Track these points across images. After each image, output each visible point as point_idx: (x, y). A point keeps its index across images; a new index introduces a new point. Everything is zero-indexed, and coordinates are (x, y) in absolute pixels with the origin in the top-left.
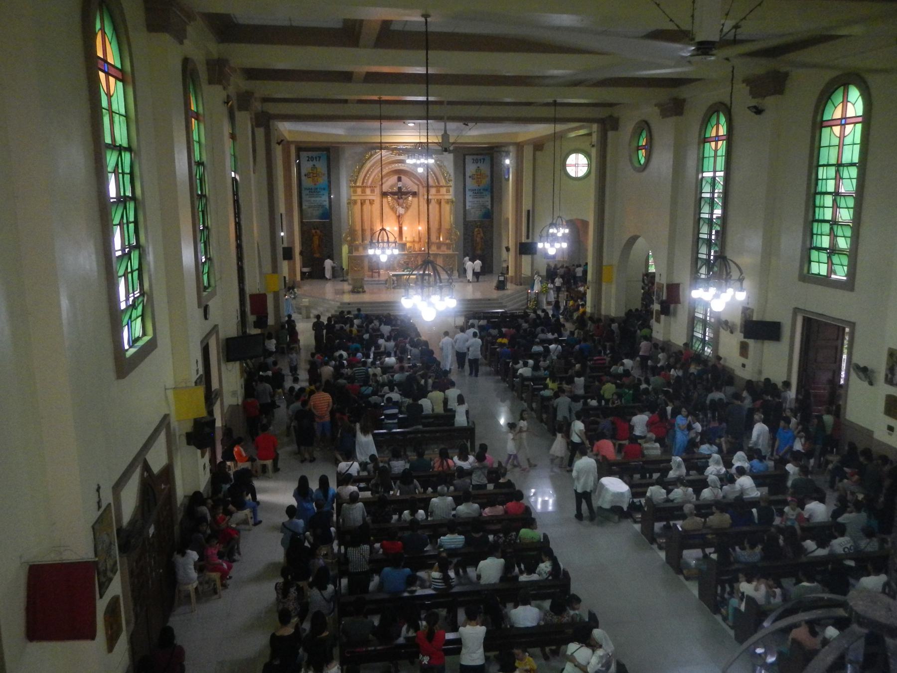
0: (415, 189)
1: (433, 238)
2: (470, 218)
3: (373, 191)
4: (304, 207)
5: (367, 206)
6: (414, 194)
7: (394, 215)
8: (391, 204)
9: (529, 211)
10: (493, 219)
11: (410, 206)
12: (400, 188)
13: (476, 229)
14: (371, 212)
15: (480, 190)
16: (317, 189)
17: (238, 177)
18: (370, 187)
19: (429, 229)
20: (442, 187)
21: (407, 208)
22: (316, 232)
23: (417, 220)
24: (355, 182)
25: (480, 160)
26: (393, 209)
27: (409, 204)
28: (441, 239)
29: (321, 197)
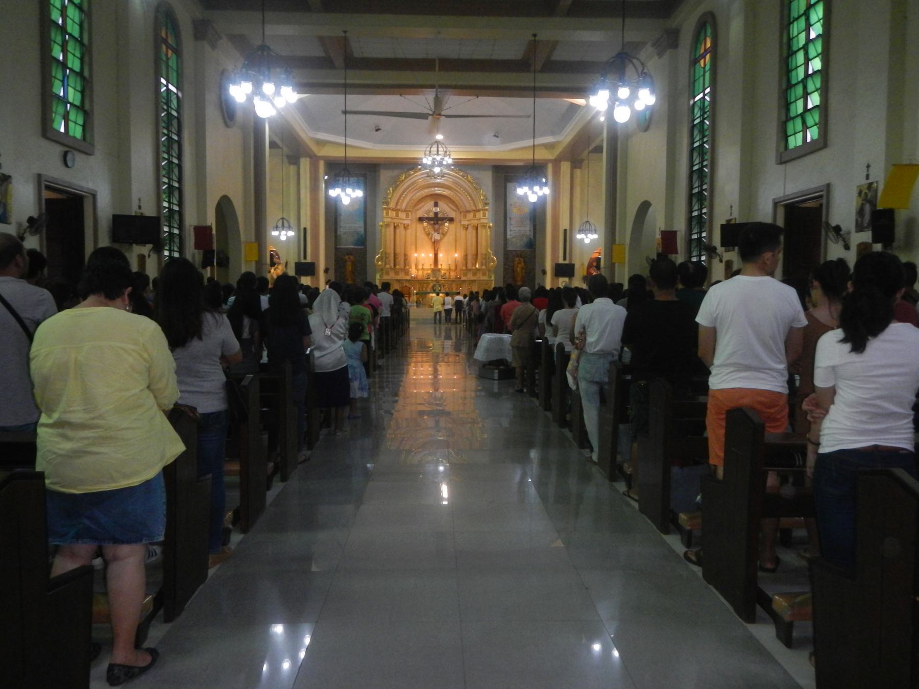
0: (452, 214)
1: (469, 266)
2: (510, 248)
3: (407, 216)
4: (339, 233)
5: (400, 231)
6: (451, 220)
8: (426, 230)
9: (565, 231)
10: (535, 248)
11: (447, 232)
12: (436, 214)
13: (517, 259)
14: (405, 237)
17: (180, 95)
18: (405, 211)
19: (466, 256)
20: (479, 211)
21: (444, 235)
22: (349, 258)
23: (454, 247)
24: (388, 205)
26: (428, 234)
27: (446, 231)
28: (477, 266)
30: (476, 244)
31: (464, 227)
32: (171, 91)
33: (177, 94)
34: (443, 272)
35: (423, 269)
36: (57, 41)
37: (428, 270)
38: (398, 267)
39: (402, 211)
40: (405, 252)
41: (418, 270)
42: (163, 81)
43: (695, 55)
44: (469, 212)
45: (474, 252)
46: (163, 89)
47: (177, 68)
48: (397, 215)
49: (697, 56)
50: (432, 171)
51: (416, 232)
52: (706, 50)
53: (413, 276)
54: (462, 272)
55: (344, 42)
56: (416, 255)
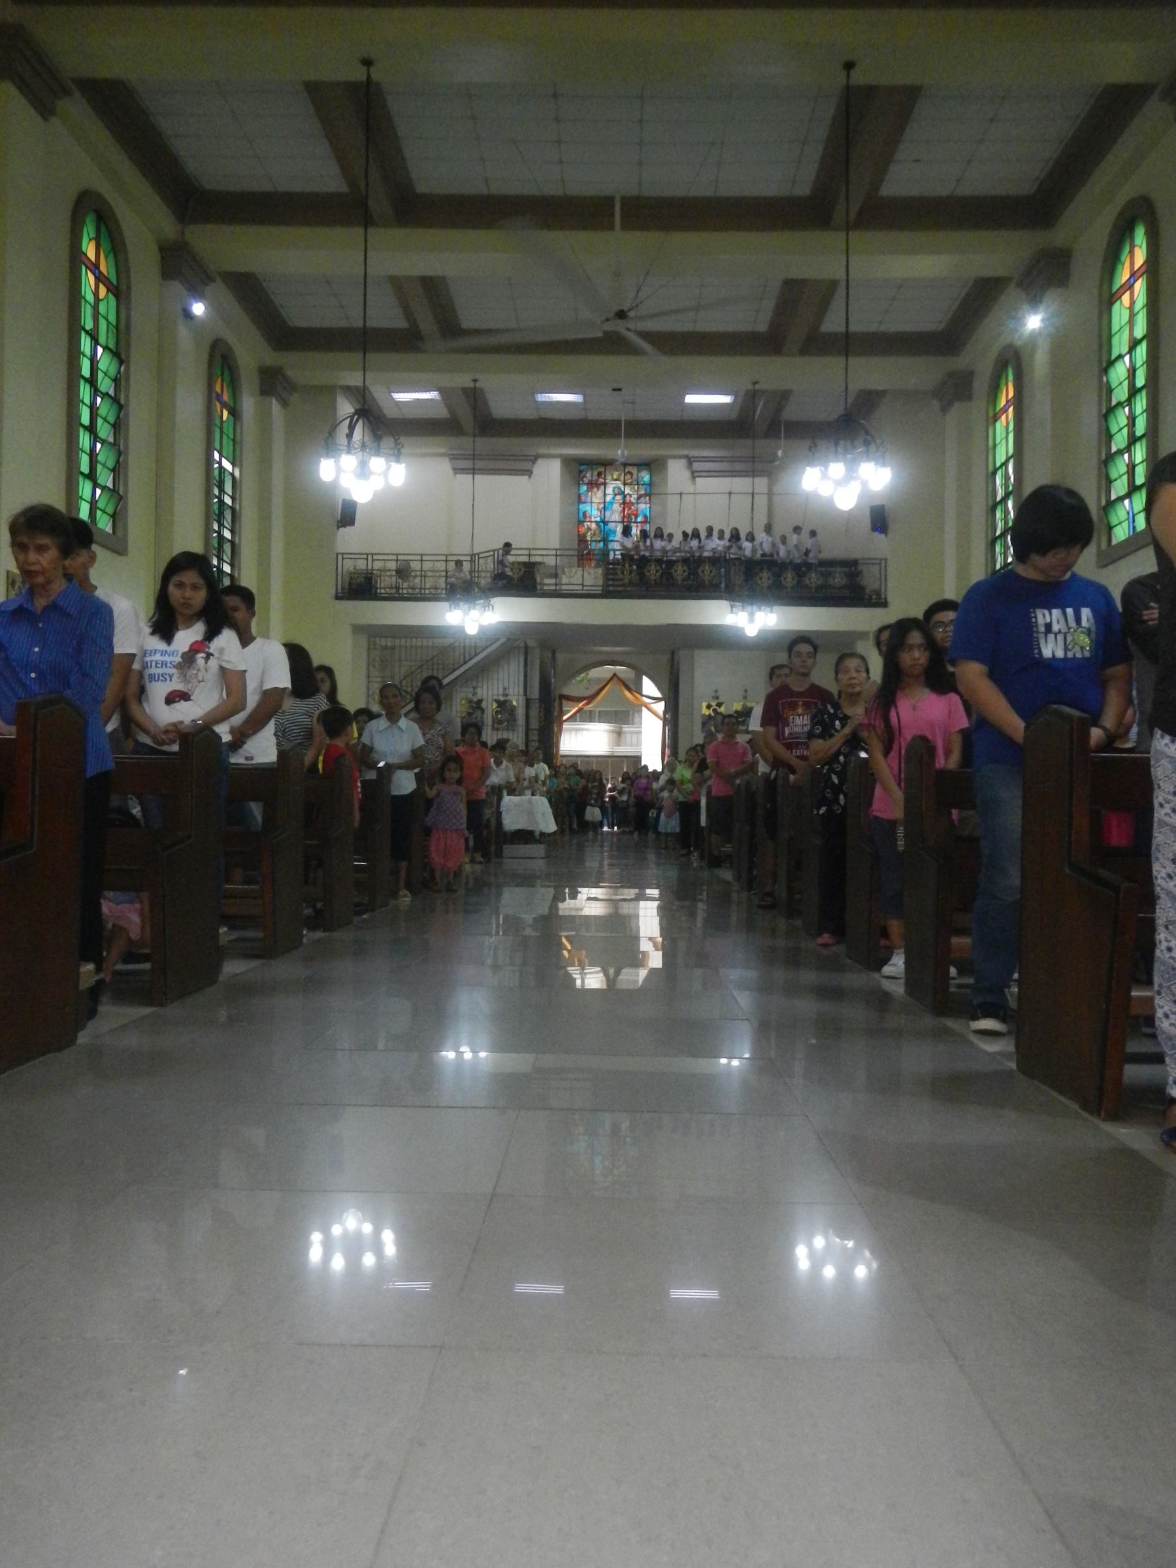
17: (237, 473)
32: (225, 469)
33: (232, 475)
36: (85, 401)
42: (216, 456)
43: (995, 410)
46: (216, 466)
47: (234, 436)
49: (997, 410)
52: (1007, 402)
55: (474, 396)
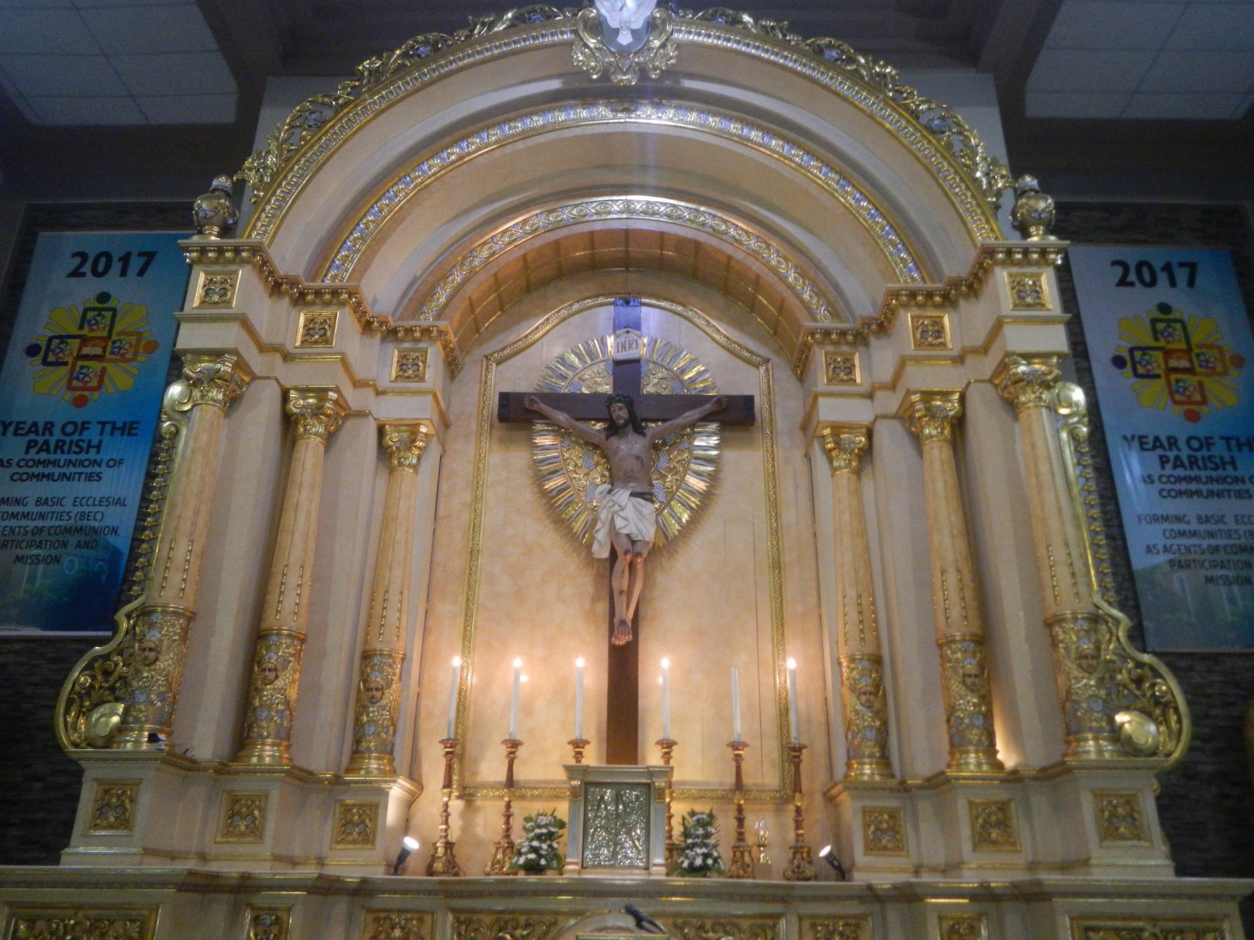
3: (409, 368)
7: (572, 564)
15: (1207, 443)
16: (84, 426)
25: (1168, 268)
27: (699, 485)
28: (1006, 756)
29: (90, 477)
30: (961, 545)
31: (838, 443)
34: (679, 809)
35: (510, 783)
37: (549, 791)
38: (267, 753)
39: (367, 327)
40: (366, 642)
41: (467, 795)
44: (882, 326)
45: (959, 623)
48: (318, 334)
50: (598, 27)
51: (477, 499)
53: (411, 843)
54: (850, 807)
56: (457, 661)
